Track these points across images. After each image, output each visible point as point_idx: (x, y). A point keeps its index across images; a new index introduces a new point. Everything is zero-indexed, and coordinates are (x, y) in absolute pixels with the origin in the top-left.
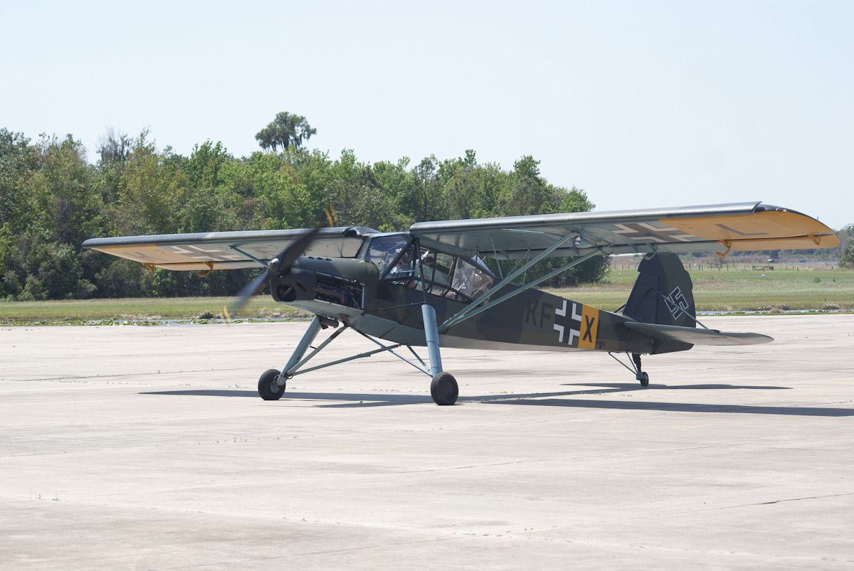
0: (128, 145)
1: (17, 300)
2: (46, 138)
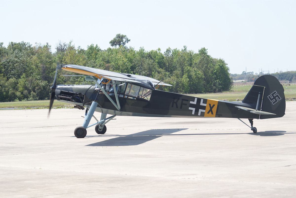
0: (66, 46)
1: (28, 100)
2: (37, 44)
